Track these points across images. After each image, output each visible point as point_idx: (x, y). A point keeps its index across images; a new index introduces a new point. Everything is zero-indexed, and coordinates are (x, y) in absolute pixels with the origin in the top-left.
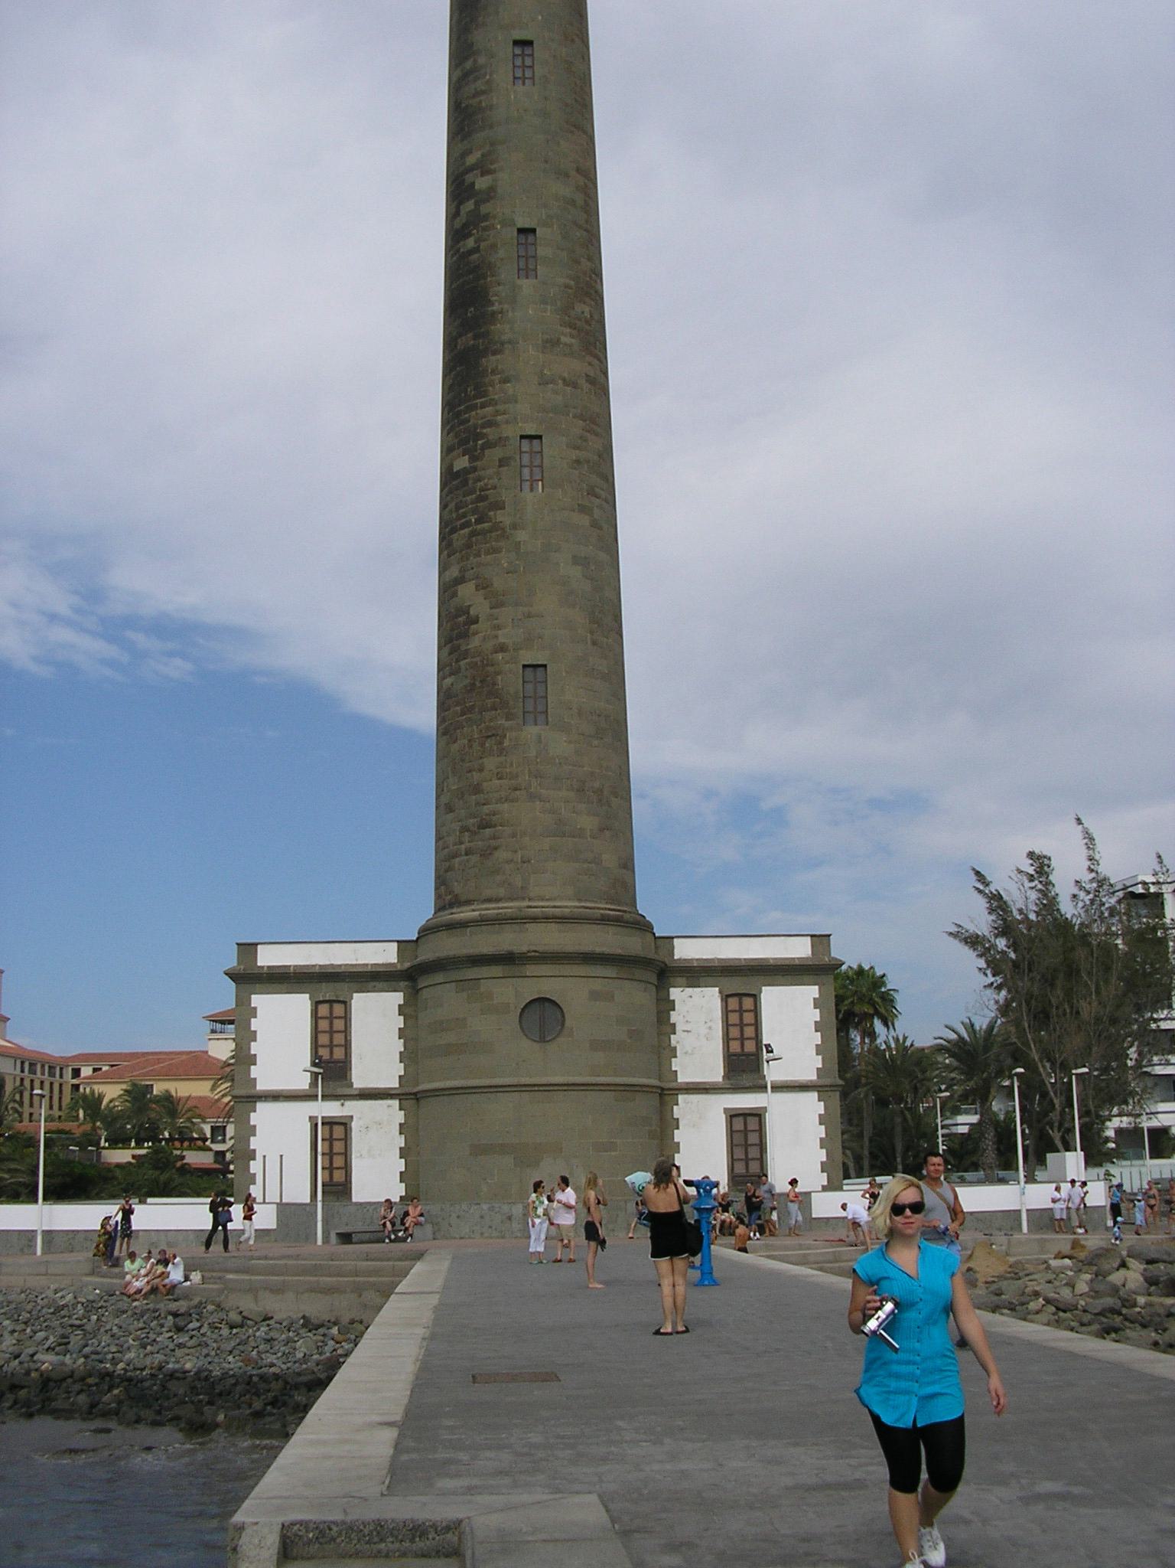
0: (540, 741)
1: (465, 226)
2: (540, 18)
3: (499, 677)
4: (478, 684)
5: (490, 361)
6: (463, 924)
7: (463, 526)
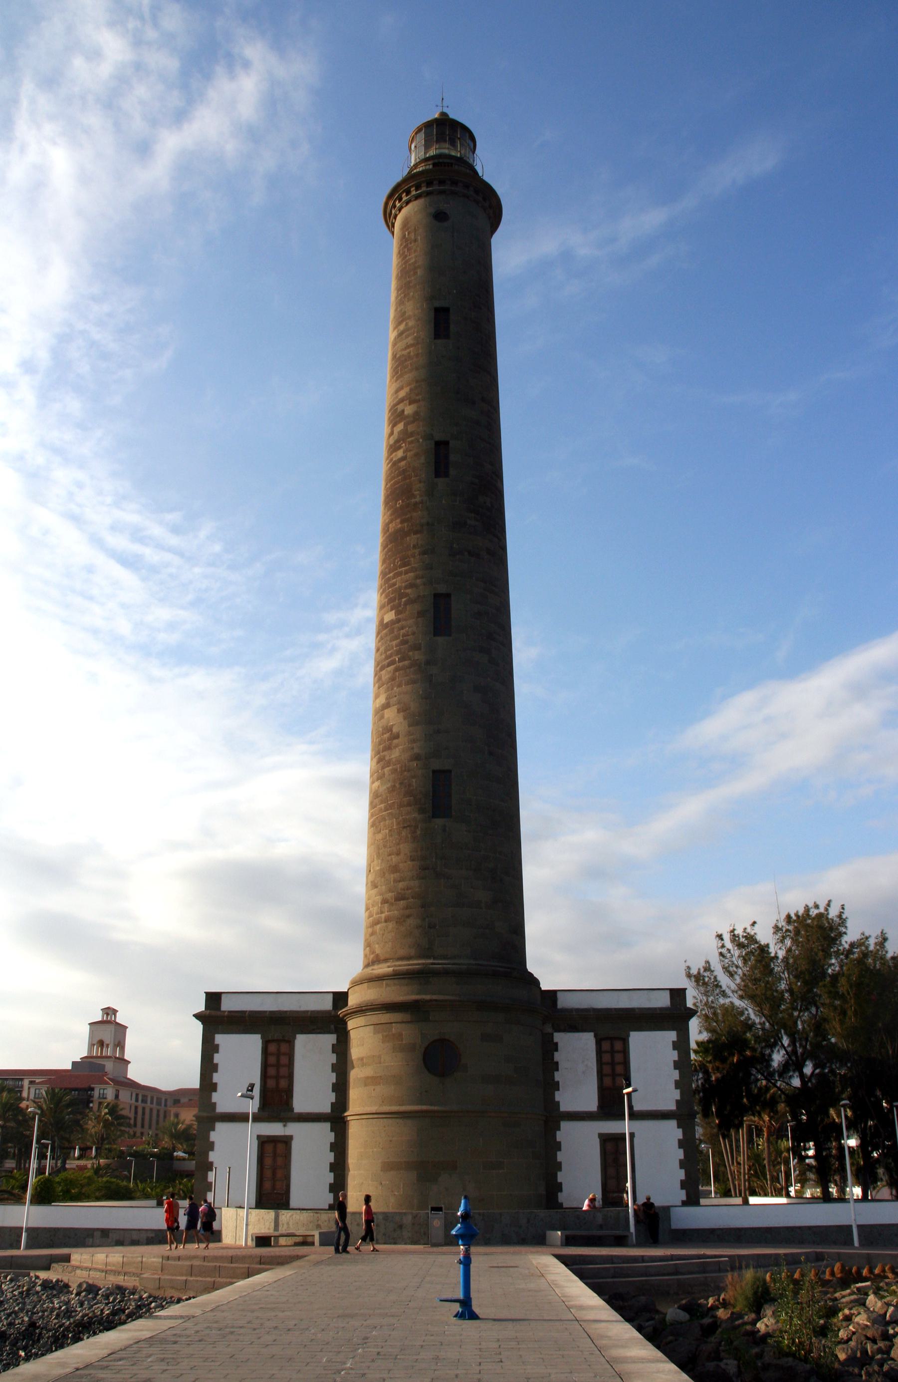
2: (455, 291)
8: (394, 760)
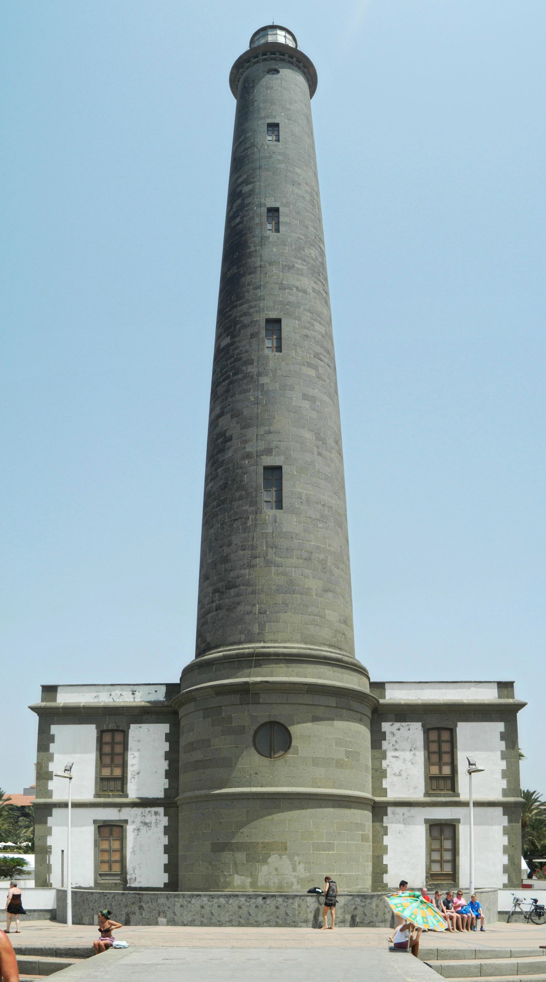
0: (275, 521)
7: (224, 380)
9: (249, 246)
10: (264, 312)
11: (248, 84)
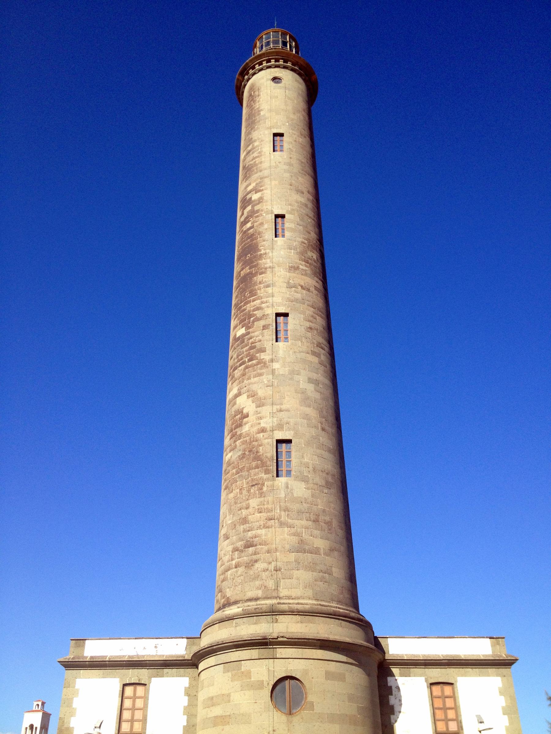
0: (287, 487)
1: (247, 218)
3: (261, 448)
4: (247, 453)
5: (259, 278)
6: (230, 618)
7: (240, 365)
8: (244, 434)
9: (259, 249)
10: (274, 307)
11: (254, 92)
